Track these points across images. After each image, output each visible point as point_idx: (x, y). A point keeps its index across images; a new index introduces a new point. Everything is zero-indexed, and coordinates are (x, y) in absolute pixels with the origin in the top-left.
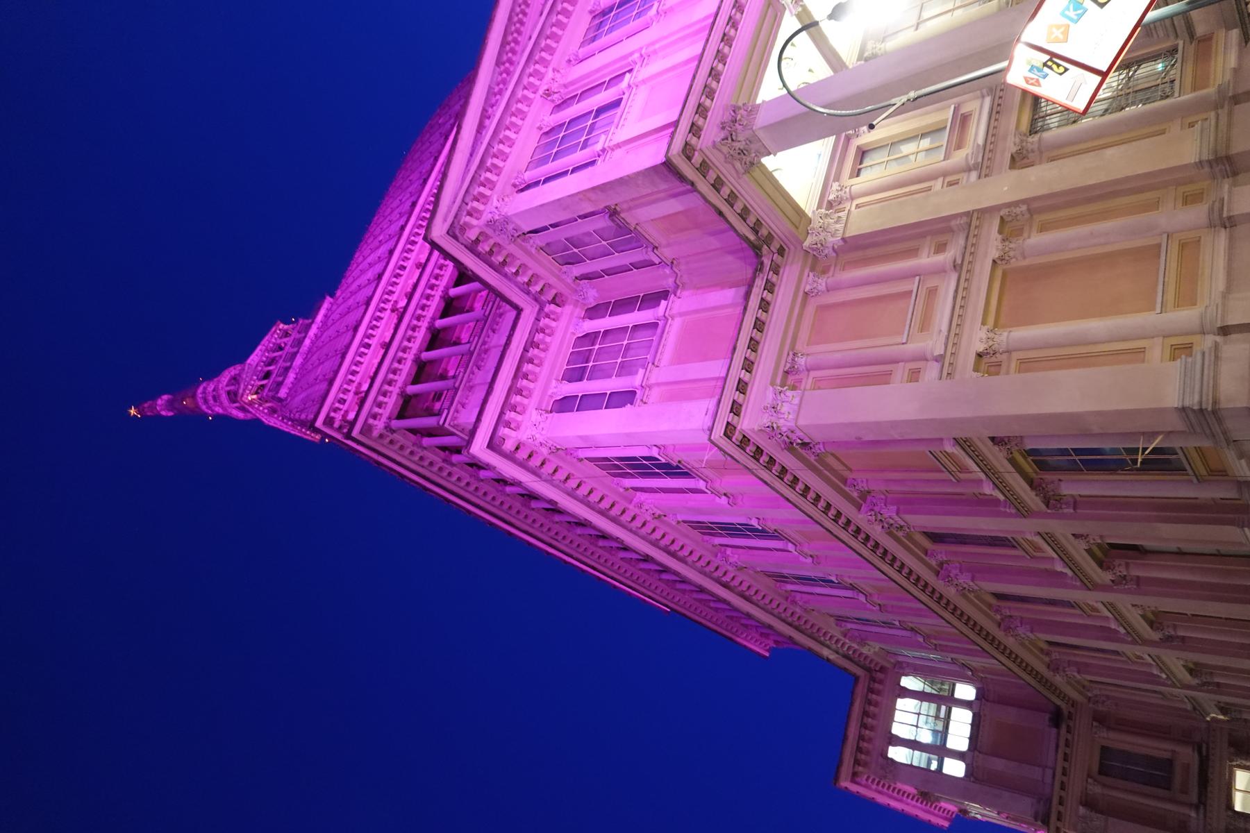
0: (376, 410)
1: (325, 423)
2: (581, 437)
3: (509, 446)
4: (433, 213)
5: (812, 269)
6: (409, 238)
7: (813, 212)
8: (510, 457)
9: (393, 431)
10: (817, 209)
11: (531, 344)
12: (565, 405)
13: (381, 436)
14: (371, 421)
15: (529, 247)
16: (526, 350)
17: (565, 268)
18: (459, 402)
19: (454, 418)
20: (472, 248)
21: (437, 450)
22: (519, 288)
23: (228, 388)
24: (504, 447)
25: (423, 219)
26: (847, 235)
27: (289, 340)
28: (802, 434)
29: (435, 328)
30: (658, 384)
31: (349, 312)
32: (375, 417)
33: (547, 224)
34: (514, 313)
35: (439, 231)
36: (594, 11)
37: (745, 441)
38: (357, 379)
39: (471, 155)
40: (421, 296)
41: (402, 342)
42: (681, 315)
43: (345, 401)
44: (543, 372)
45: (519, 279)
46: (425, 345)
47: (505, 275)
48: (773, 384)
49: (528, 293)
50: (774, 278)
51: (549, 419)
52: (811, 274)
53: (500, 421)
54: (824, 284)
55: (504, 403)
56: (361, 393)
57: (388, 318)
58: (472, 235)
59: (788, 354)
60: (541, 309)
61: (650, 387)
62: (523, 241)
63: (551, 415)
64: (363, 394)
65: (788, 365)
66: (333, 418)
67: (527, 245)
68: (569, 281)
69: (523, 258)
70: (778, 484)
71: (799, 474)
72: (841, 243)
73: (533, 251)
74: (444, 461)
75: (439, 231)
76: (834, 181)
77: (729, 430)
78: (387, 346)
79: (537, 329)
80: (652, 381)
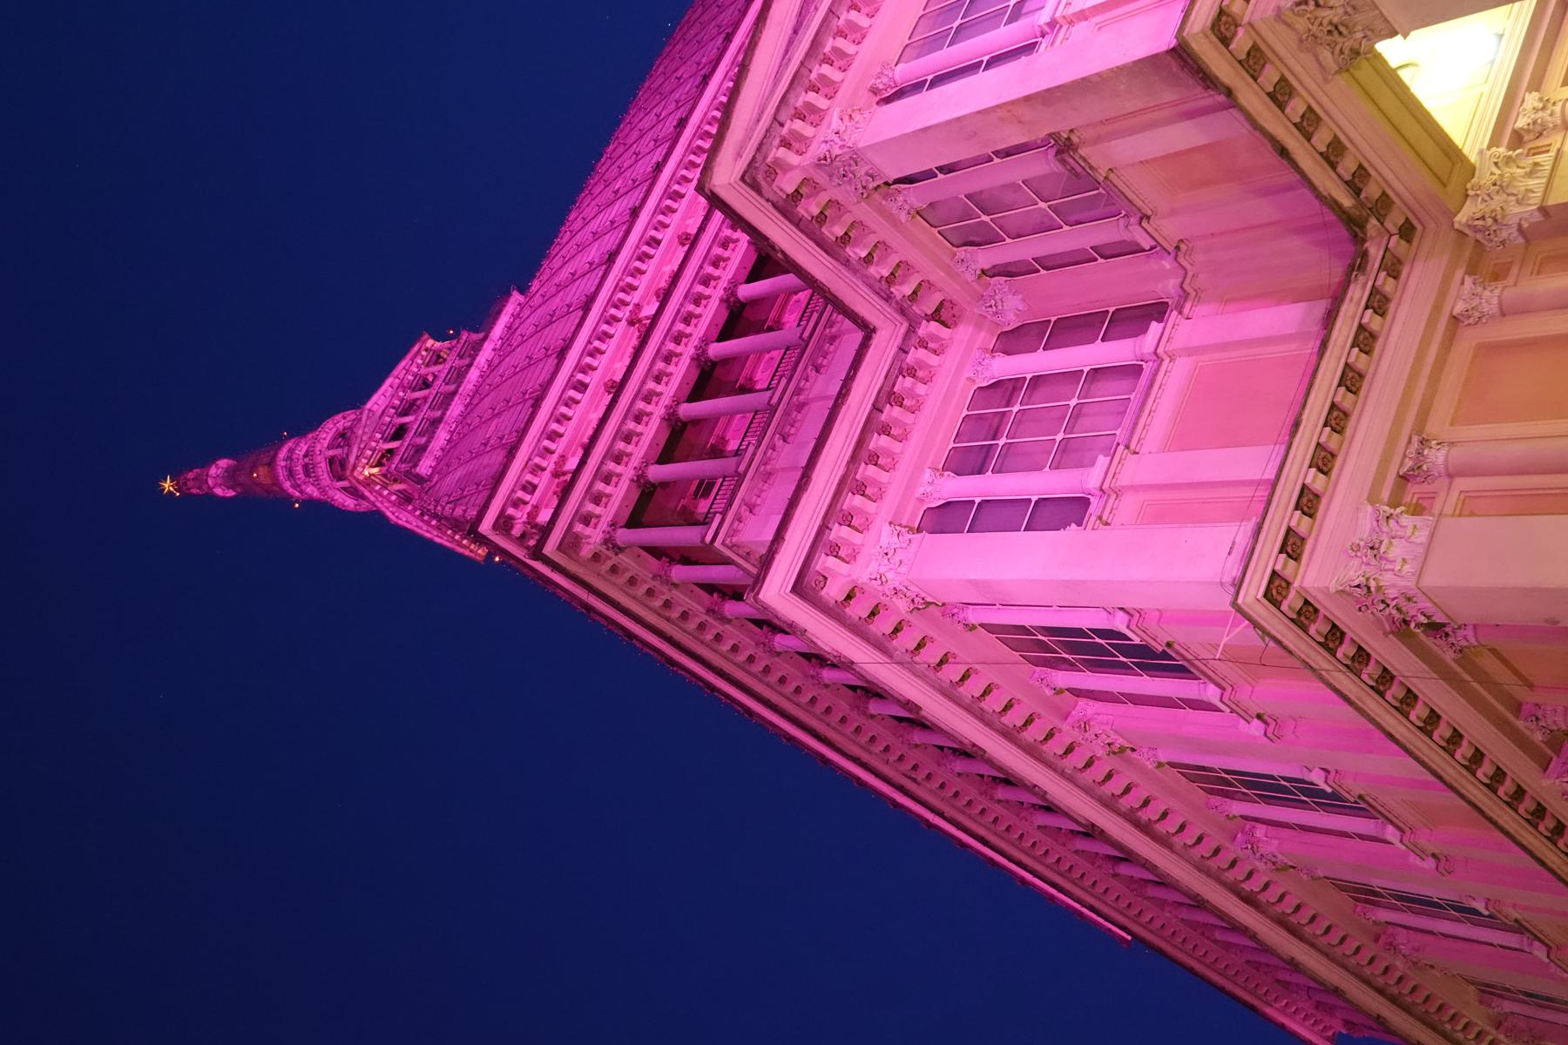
0: (590, 507)
1: (496, 526)
2: (975, 584)
3: (833, 591)
4: (719, 140)
5: (1472, 270)
7: (1481, 152)
8: (834, 612)
9: (618, 550)
10: (1489, 147)
11: (888, 396)
13: (596, 557)
14: (579, 528)
15: (894, 211)
16: (877, 408)
17: (962, 252)
19: (733, 532)
20: (786, 208)
21: (697, 589)
22: (871, 287)
23: (331, 453)
24: (823, 593)
25: (699, 151)
26: (1551, 201)
28: (1429, 604)
29: (708, 360)
30: (1135, 488)
31: (551, 323)
32: (587, 520)
33: (932, 166)
34: (858, 336)
35: (726, 176)
37: (1307, 613)
38: (559, 447)
39: (795, 32)
40: (686, 297)
41: (643, 382)
42: (1190, 351)
43: (535, 487)
44: (908, 453)
45: (872, 270)
46: (687, 390)
47: (846, 263)
48: (1372, 499)
49: (888, 298)
50: (1389, 286)
51: (914, 546)
52: (1468, 280)
54: (1495, 301)
55: (830, 506)
56: (564, 474)
57: (623, 336)
58: (788, 184)
59: (1409, 442)
60: (911, 330)
61: (1118, 493)
62: (885, 197)
63: (919, 536)
64: (568, 477)
65: (1409, 464)
66: (512, 518)
67: (892, 207)
68: (969, 277)
69: (881, 230)
70: (1372, 704)
71: (1419, 687)
72: (1538, 217)
73: (903, 217)
74: (710, 611)
75: (726, 176)
76: (1529, 90)
77: (1276, 588)
78: (617, 389)
80: (1124, 479)
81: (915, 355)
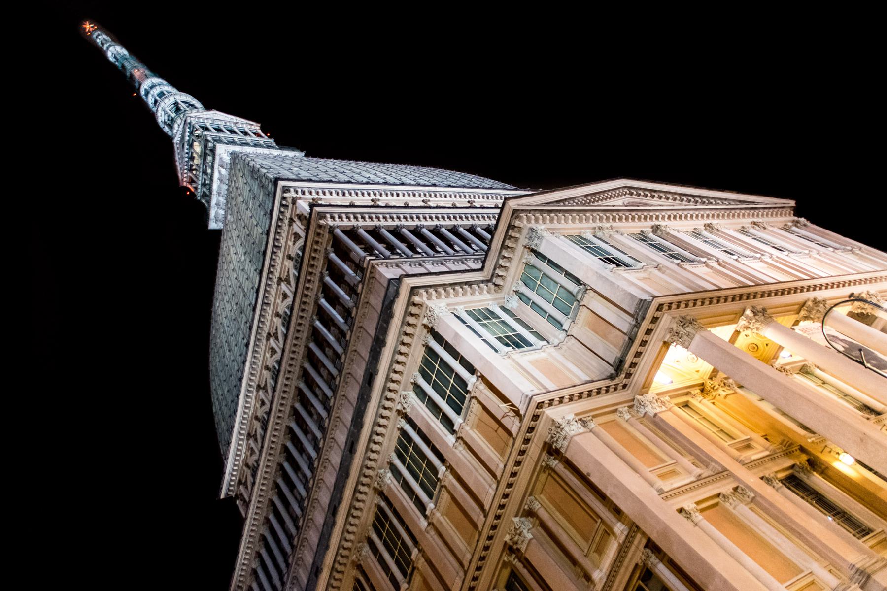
1: (284, 187)
8: (410, 303)
11: (469, 284)
13: (320, 226)
15: (525, 257)
17: (520, 282)
18: (387, 262)
20: (511, 227)
22: (496, 262)
23: (180, 102)
24: (414, 297)
26: (660, 415)
27: (254, 137)
29: (356, 231)
31: (341, 173)
35: (512, 204)
36: (643, 233)
38: (433, 198)
48: (576, 415)
50: (611, 390)
52: (627, 408)
57: (366, 200)
58: (517, 223)
59: (589, 417)
66: (289, 191)
69: (516, 257)
72: (652, 415)
76: (669, 396)
77: (540, 405)
79: (477, 283)
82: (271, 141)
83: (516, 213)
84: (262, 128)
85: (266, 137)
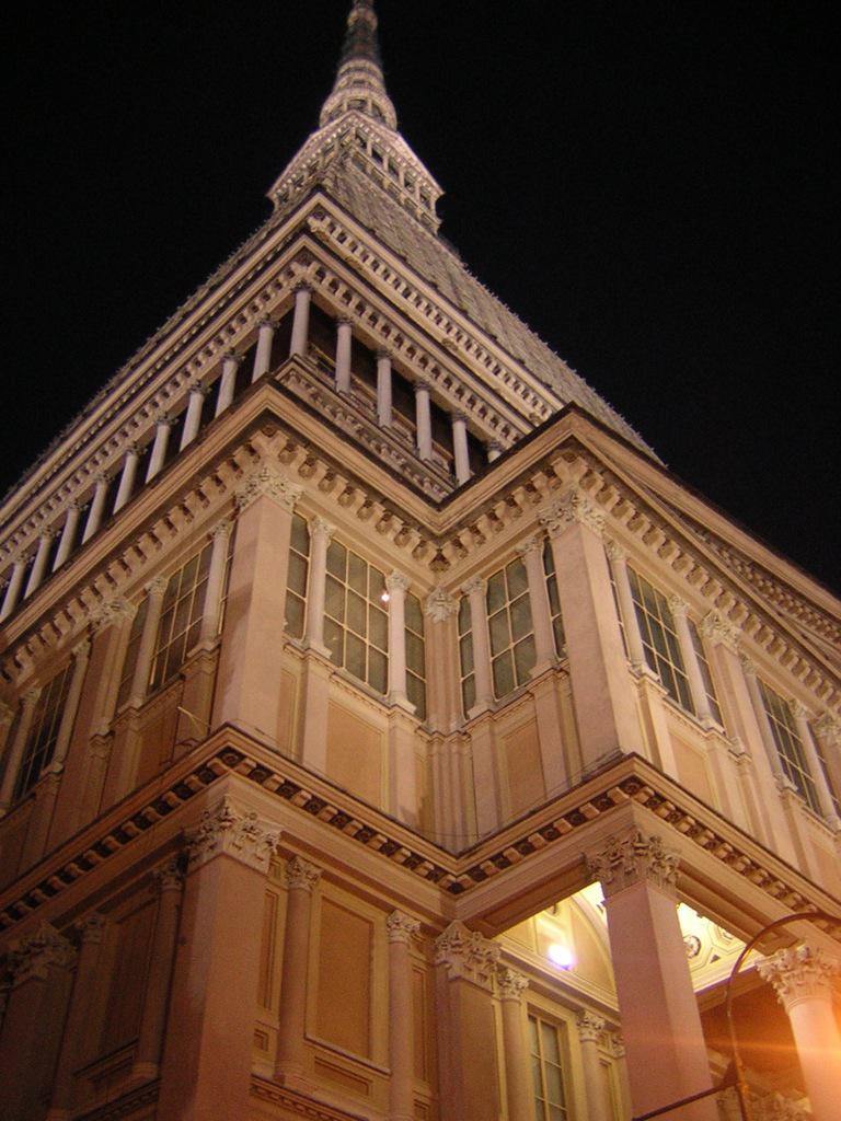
1: (318, 205)
2: (254, 544)
3: (259, 440)
5: (424, 928)
6: (534, 391)
7: (500, 945)
8: (243, 439)
10: (503, 952)
12: (302, 536)
13: (291, 274)
16: (384, 500)
21: (250, 345)
23: (370, 104)
27: (416, 198)
28: (205, 861)
30: (305, 674)
34: (438, 498)
35: (577, 427)
36: (793, 706)
37: (208, 775)
39: (659, 497)
40: (464, 383)
41: (411, 338)
42: (392, 730)
43: (342, 242)
44: (349, 514)
48: (284, 835)
49: (460, 525)
51: (284, 505)
53: (298, 437)
55: (323, 451)
60: (432, 536)
61: (304, 660)
62: (538, 536)
63: (291, 512)
65: (302, 864)
67: (530, 538)
69: (513, 527)
70: (126, 810)
71: (132, 847)
73: (519, 546)
74: (233, 350)
75: (577, 427)
76: (530, 981)
79: (409, 522)
80: (312, 666)
81: (416, 537)
82: (436, 222)
83: (573, 447)
84: (439, 203)
85: (434, 212)
